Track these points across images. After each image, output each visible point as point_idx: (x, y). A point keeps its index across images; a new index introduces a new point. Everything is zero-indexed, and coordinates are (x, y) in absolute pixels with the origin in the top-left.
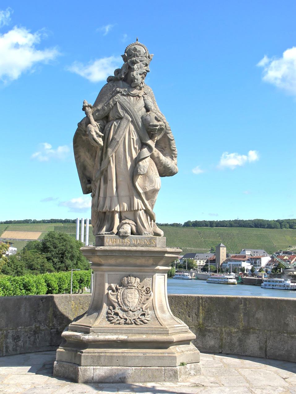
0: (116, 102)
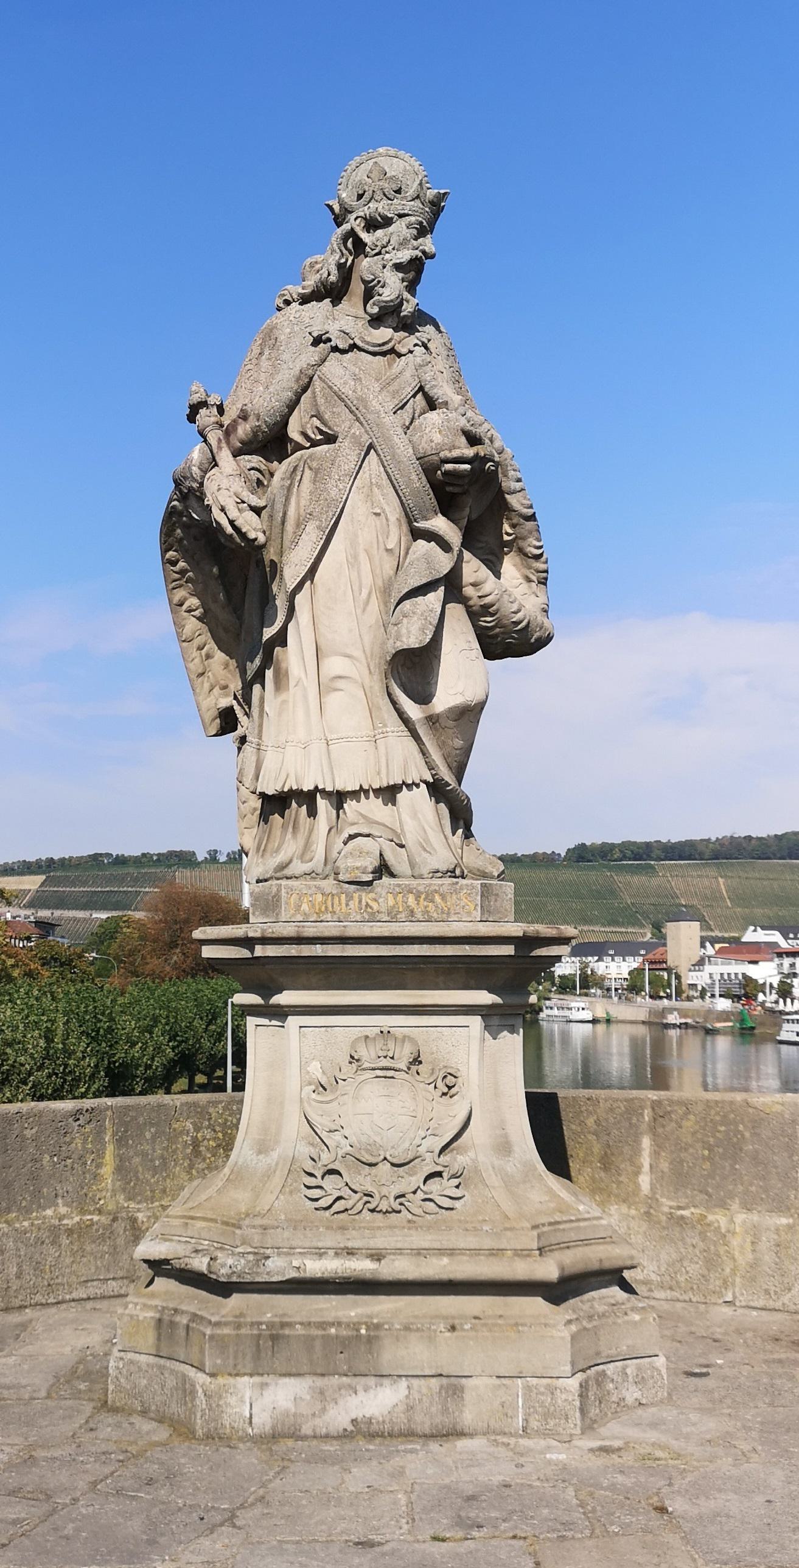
0: (311, 378)
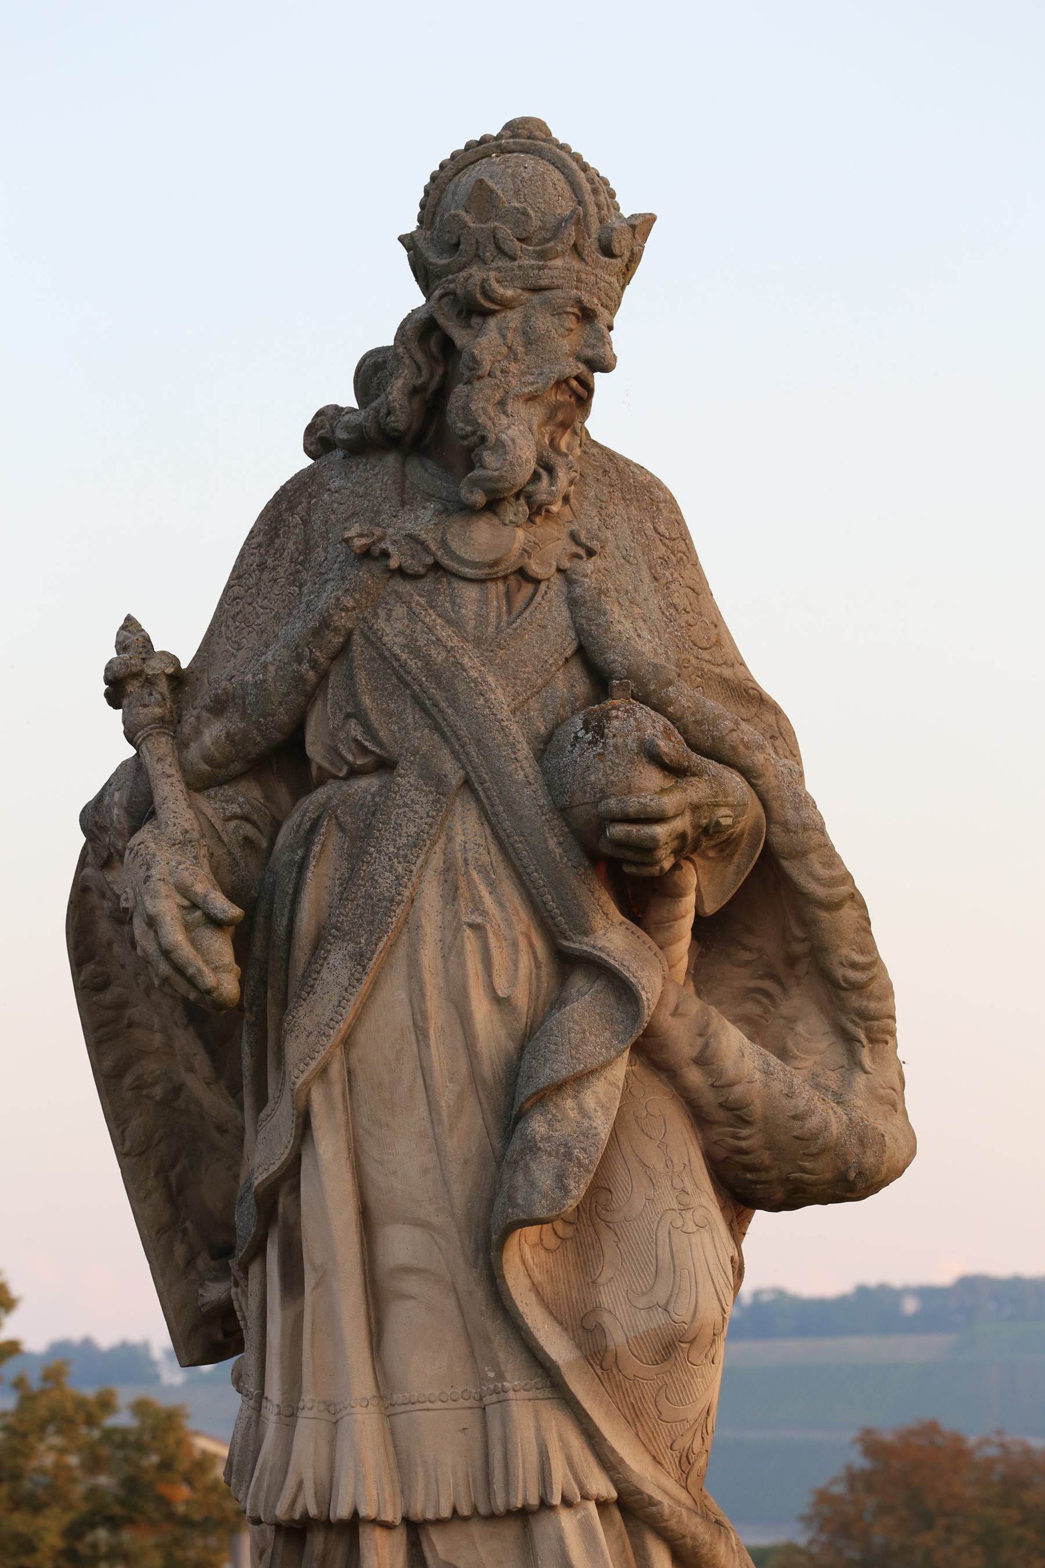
0: (350, 634)
